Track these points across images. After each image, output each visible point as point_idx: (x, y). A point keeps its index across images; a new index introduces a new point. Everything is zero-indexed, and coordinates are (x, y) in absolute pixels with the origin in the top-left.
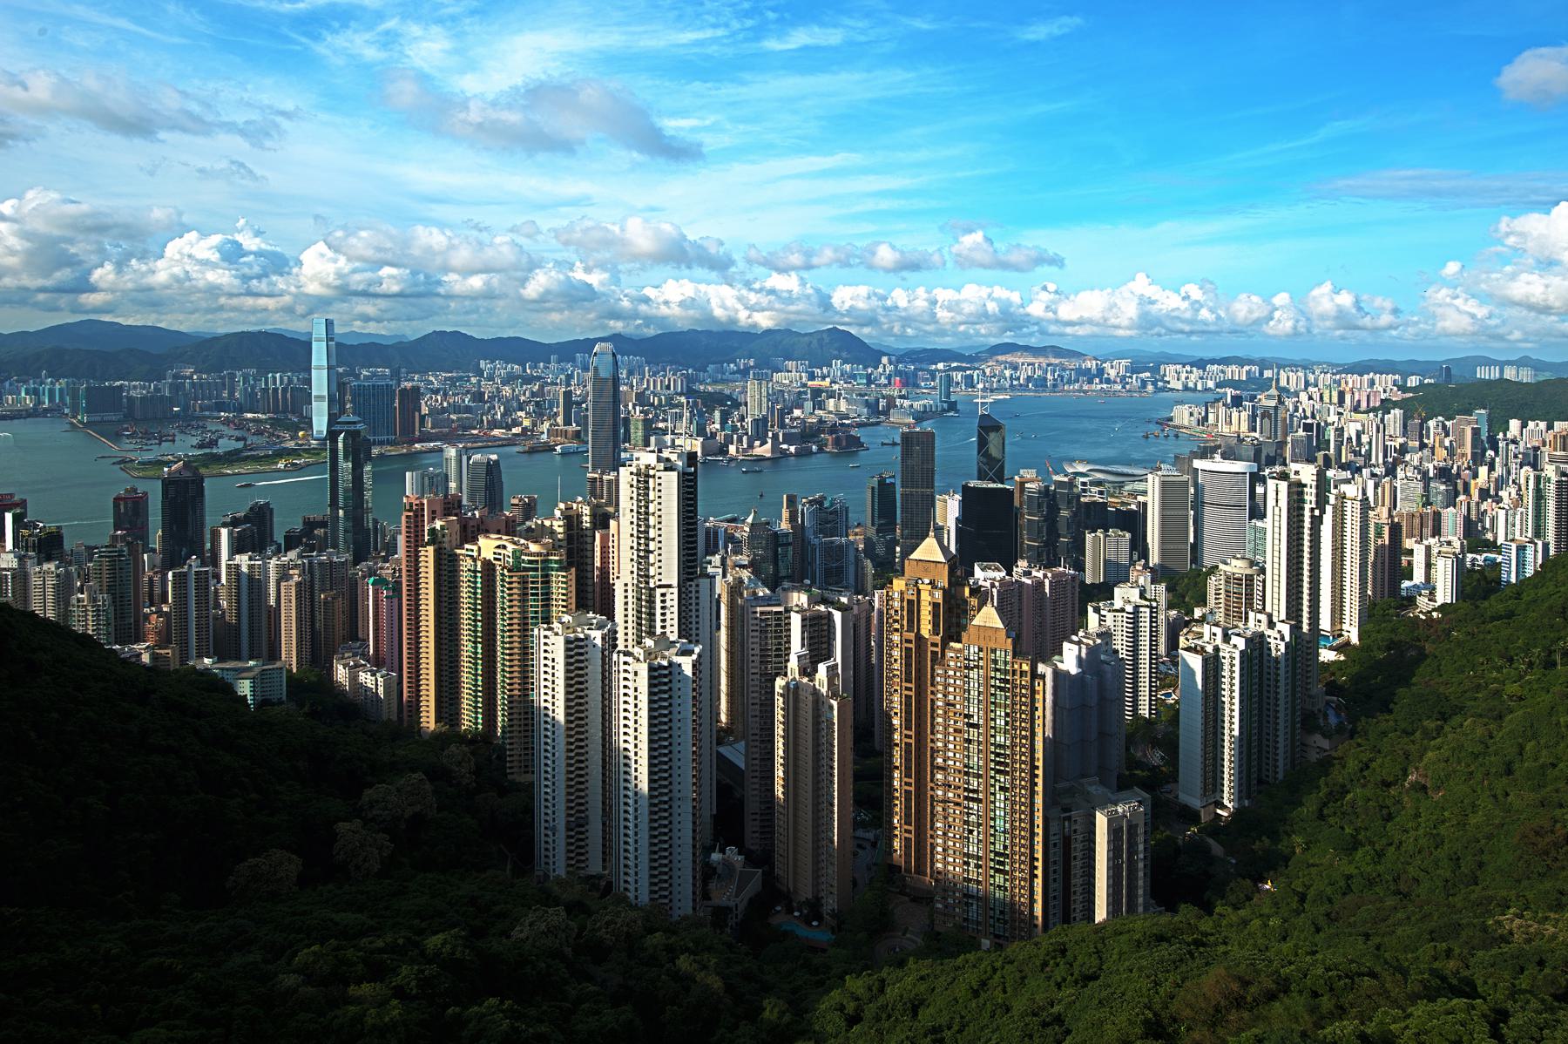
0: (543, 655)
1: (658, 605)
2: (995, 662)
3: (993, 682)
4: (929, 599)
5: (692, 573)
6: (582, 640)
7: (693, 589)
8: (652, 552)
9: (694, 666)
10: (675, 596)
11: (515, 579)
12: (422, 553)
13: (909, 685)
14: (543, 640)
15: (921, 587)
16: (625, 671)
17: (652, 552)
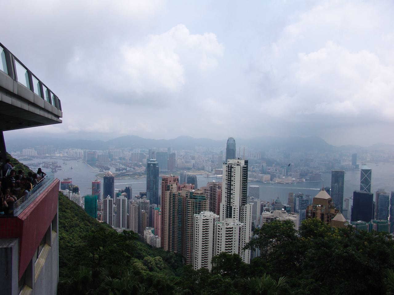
0: (196, 224)
1: (233, 212)
4: (320, 212)
5: (245, 203)
6: (207, 219)
7: (245, 208)
8: (232, 194)
9: (240, 229)
10: (238, 210)
11: (190, 201)
12: (166, 193)
14: (196, 219)
15: (317, 208)
16: (219, 229)
17: (232, 194)
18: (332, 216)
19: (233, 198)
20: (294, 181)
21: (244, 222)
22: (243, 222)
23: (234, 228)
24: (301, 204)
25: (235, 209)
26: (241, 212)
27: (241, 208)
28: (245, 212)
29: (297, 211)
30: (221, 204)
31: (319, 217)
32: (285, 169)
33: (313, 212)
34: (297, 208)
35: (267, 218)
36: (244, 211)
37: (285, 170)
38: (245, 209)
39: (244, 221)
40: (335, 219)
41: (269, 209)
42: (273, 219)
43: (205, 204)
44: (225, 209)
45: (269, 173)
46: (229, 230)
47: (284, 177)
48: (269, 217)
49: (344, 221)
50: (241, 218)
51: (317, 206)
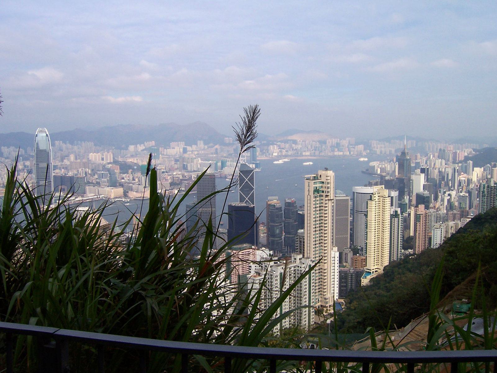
45: (121, 185)
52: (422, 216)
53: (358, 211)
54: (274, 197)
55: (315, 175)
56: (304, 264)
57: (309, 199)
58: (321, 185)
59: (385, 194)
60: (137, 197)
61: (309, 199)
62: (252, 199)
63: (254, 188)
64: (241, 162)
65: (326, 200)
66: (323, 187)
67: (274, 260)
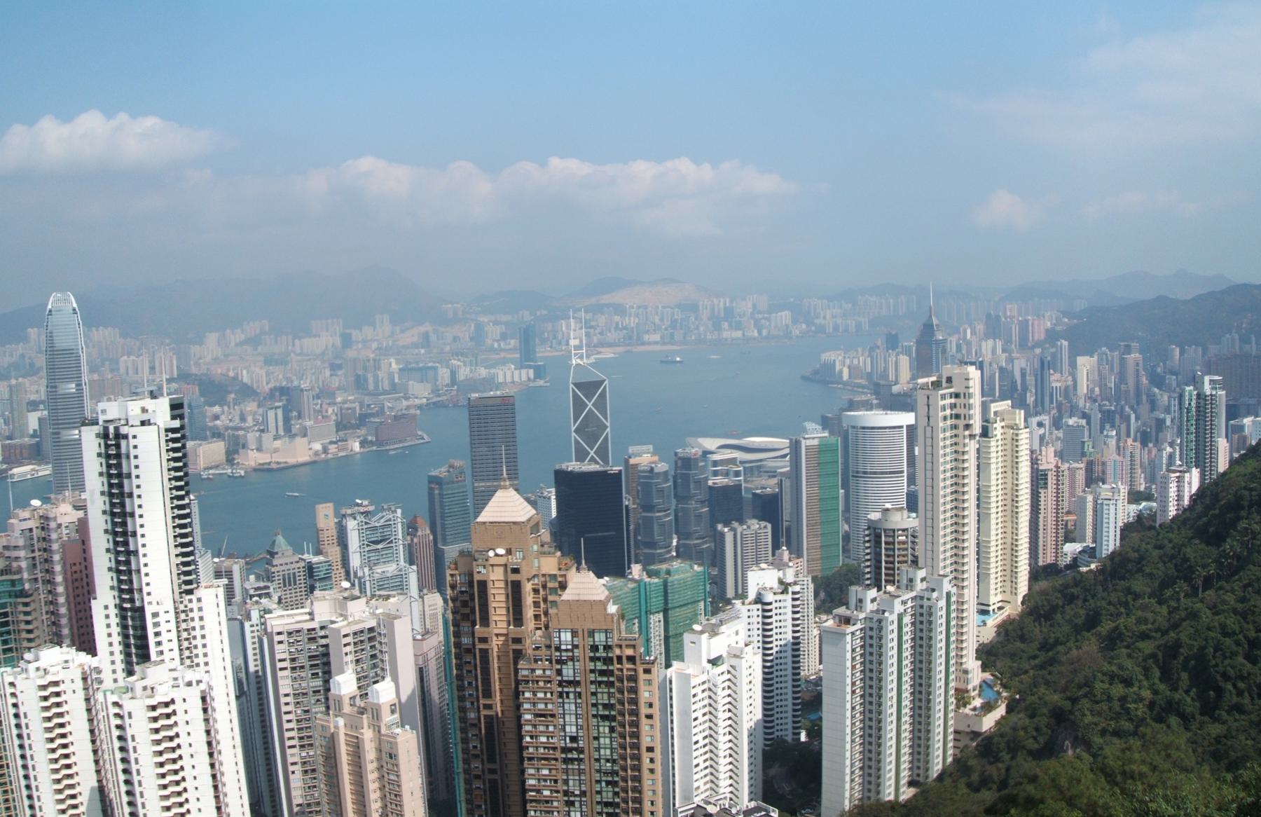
1: (151, 631)
2: (594, 648)
3: (592, 677)
7: (195, 605)
9: (204, 699)
10: (172, 616)
13: (488, 702)
15: (491, 562)
18: (550, 585)
19: (144, 570)
20: (316, 453)
21: (202, 665)
22: (198, 665)
23: (179, 702)
24: (368, 545)
25: (155, 615)
26: (184, 626)
27: (182, 607)
28: (197, 623)
29: (355, 574)
30: (93, 602)
31: (503, 598)
32: (277, 408)
33: (478, 581)
34: (355, 561)
35: (290, 634)
36: (193, 619)
37: (280, 412)
38: (196, 610)
39: (201, 660)
40: (567, 595)
41: (267, 587)
42: (314, 629)
43: (26, 613)
44: (114, 620)
46: (163, 712)
47: (278, 443)
48: (298, 626)
49: (602, 597)
50: (188, 648)
51: (491, 553)
52: (1050, 473)
53: (857, 472)
54: (645, 448)
55: (934, 379)
56: (933, 590)
57: (929, 434)
58: (953, 401)
59: (1017, 422)
60: (260, 464)
61: (929, 434)
62: (603, 453)
63: (608, 424)
64: (574, 362)
65: (964, 437)
66: (958, 406)
67: (794, 593)
